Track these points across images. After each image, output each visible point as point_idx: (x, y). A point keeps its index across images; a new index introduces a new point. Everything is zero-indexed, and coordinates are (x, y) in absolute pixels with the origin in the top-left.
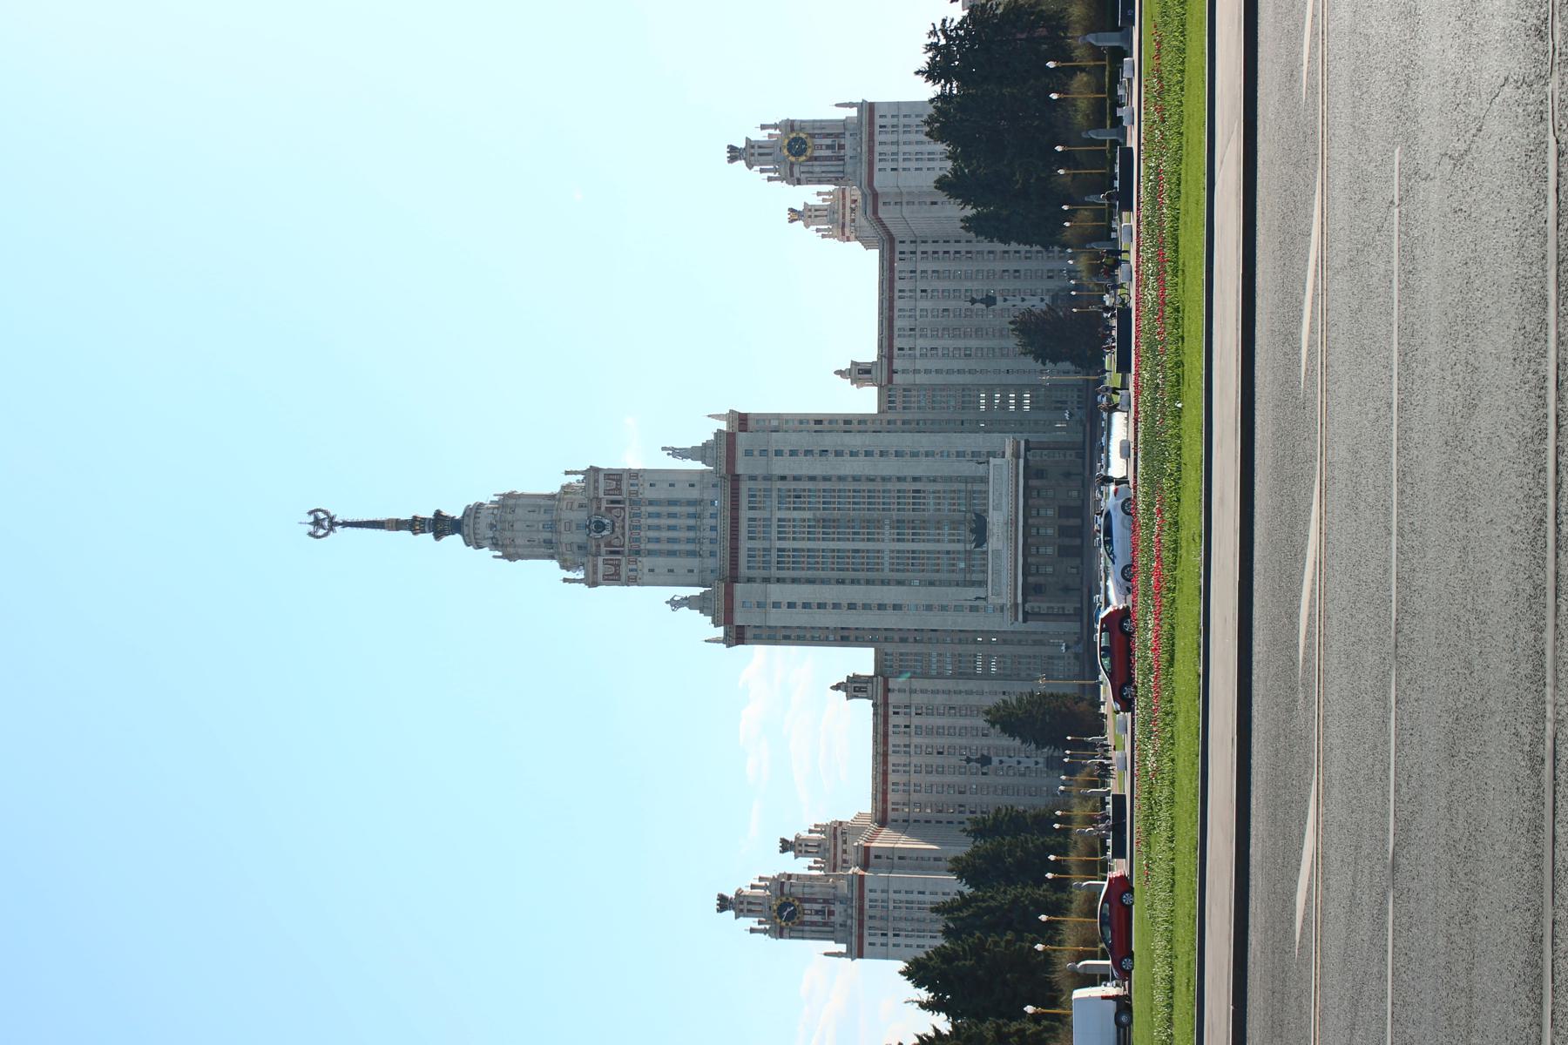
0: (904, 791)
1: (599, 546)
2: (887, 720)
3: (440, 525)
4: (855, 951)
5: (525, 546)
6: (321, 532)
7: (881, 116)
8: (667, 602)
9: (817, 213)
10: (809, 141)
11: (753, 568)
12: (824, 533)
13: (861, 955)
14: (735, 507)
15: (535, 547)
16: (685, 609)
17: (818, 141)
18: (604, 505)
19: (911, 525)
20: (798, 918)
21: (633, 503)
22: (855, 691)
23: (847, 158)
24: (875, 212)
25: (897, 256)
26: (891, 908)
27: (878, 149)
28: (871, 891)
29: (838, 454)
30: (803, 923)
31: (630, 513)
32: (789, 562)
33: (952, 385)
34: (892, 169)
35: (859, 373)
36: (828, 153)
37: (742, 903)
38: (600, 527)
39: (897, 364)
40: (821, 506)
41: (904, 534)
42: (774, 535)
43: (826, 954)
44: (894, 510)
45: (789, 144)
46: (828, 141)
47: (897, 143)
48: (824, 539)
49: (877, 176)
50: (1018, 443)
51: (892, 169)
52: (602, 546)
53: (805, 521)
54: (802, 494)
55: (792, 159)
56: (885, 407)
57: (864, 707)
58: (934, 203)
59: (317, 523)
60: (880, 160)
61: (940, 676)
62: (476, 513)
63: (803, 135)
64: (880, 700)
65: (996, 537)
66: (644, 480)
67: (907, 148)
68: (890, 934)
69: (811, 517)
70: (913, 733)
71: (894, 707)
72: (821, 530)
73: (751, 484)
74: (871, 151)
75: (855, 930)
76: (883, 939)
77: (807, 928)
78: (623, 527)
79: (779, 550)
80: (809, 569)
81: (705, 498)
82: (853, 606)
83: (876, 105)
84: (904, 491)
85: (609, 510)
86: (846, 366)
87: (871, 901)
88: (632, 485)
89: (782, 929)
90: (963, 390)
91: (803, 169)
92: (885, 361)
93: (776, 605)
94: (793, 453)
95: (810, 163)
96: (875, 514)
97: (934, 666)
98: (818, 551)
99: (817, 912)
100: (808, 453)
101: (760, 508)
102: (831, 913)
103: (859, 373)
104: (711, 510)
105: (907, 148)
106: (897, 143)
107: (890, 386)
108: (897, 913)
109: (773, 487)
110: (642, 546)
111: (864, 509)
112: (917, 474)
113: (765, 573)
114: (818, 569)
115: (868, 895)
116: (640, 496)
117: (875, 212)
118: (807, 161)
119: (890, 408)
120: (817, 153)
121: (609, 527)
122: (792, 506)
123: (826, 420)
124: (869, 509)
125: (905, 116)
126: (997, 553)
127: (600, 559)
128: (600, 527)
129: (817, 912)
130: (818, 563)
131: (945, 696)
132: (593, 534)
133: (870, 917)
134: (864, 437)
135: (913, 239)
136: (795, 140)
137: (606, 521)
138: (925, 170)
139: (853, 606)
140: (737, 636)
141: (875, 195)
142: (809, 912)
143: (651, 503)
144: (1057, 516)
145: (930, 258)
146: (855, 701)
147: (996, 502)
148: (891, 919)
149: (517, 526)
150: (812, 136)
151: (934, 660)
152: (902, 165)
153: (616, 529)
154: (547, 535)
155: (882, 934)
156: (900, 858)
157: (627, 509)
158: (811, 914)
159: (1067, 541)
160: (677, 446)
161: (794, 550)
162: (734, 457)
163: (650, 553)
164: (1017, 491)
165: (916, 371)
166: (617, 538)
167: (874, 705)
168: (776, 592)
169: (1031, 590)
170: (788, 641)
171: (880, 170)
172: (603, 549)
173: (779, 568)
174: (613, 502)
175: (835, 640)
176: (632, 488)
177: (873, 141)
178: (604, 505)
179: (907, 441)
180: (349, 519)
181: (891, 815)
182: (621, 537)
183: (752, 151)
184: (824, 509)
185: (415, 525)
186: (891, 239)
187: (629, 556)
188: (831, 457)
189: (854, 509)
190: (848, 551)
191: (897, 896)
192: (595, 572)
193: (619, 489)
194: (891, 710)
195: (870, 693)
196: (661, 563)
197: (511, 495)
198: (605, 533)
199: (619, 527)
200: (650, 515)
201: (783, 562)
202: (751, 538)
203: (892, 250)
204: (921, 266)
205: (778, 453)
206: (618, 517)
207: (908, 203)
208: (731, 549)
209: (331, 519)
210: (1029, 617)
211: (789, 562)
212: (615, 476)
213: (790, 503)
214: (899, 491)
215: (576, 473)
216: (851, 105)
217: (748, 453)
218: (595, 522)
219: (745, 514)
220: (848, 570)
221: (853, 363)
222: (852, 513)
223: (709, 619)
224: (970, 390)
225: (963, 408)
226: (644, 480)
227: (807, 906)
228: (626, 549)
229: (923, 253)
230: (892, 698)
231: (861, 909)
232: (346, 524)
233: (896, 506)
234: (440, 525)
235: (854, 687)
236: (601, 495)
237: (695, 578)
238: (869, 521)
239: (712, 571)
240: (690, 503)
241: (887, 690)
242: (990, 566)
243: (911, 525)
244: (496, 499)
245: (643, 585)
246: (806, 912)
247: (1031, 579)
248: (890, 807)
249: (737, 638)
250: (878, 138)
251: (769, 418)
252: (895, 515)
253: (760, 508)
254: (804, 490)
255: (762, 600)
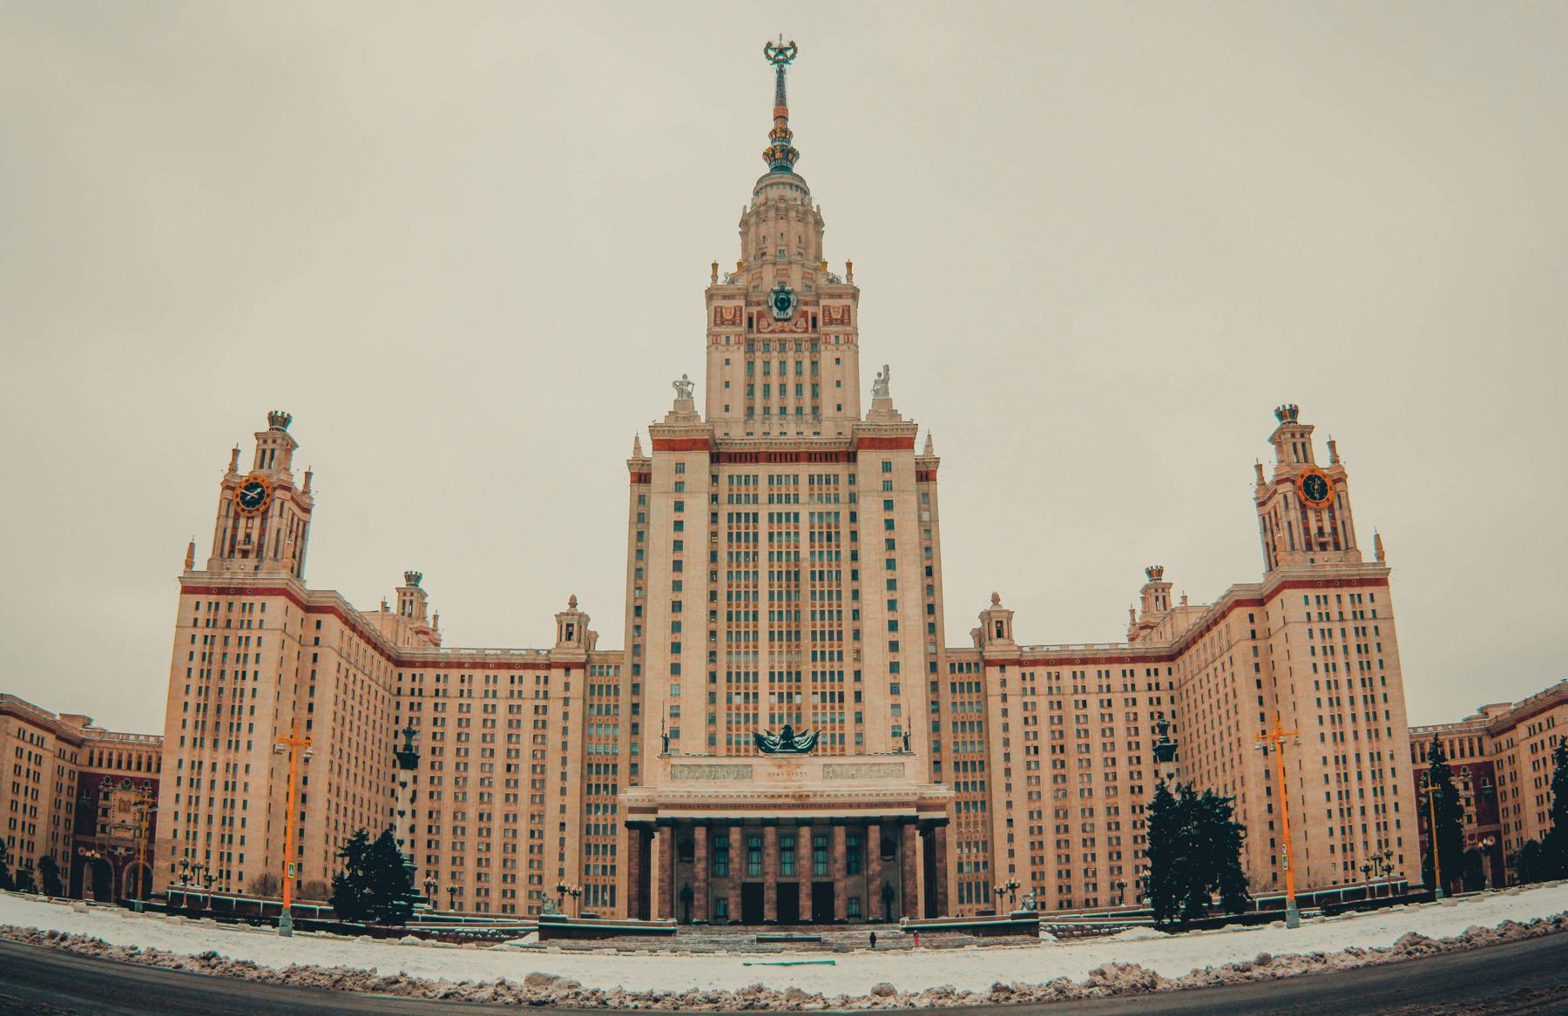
0: (437, 691)
1: (759, 304)
2: (529, 668)
3: (782, 156)
4: (189, 584)
5: (757, 234)
6: (772, 53)
7: (1372, 595)
8: (685, 377)
9: (1299, 447)
10: (1324, 504)
11: (731, 482)
12: (780, 573)
13: (186, 590)
14: (812, 457)
15: (758, 244)
16: (674, 395)
17: (1326, 516)
18: (810, 309)
19: (794, 691)
20: (243, 510)
21: (814, 344)
22: (569, 625)
23: (1310, 555)
24: (1239, 603)
25: (1152, 666)
26: (240, 633)
27: (1332, 593)
28: (263, 605)
29: (891, 585)
30: (237, 517)
31: (801, 339)
32: (739, 528)
33: (988, 748)
34: (1308, 614)
35: (996, 624)
36: (1314, 530)
37: (274, 442)
38: (783, 304)
39: (1013, 673)
40: (817, 569)
41: (781, 680)
42: (777, 508)
43: (192, 546)
44: (814, 666)
45: (1319, 478)
46: (1328, 529)
47: (1342, 619)
48: (771, 573)
49: (1298, 594)
50: (942, 807)
51: (1308, 614)
52: (759, 308)
53: (796, 547)
54: (833, 543)
55: (1300, 482)
56: (954, 659)
57: (544, 638)
58: (1259, 682)
59: (781, 51)
60: (1318, 597)
61: (586, 737)
62: (797, 187)
63: (1330, 495)
64: (555, 658)
65: (775, 770)
66: (844, 351)
67: (1337, 634)
68: (208, 632)
69: (801, 556)
70: (511, 702)
71: (546, 678)
72: (784, 569)
73: (843, 479)
74: (1328, 583)
75: (217, 582)
76: (201, 623)
77: (230, 522)
78: (782, 331)
79: (755, 515)
80: (730, 554)
81: (823, 423)
82: (676, 608)
83: (1384, 587)
84: (841, 679)
85: (805, 314)
86: (1005, 604)
87: (251, 604)
88: (837, 337)
89: (233, 489)
90: (981, 763)
91: (1290, 495)
92: (1015, 656)
93: (679, 506)
94: (890, 524)
95: (1298, 507)
96: (806, 641)
97: (602, 731)
98: (755, 566)
99: (248, 536)
100: (891, 544)
101: (812, 489)
102: (245, 554)
103: (996, 624)
104: (808, 433)
105: (1337, 634)
106: (1342, 619)
107: (981, 665)
108: (233, 641)
109: (841, 505)
110: (758, 354)
111: (814, 626)
112: (866, 697)
113: (723, 497)
114: (730, 566)
115: (257, 600)
116: (823, 347)
117: (1239, 603)
118: (1300, 502)
119: (952, 665)
120: (1311, 515)
121: (782, 317)
122: (817, 530)
123: (933, 581)
124: (814, 633)
125: (1376, 628)
126: (745, 773)
127: (742, 303)
128: (783, 304)
129: (248, 536)
130: (738, 566)
131: (560, 745)
132: (773, 297)
133: (230, 604)
134: (917, 618)
135: (1175, 686)
136: (1323, 485)
137: (790, 311)
138: (1313, 660)
139: (676, 608)
140: (641, 477)
141: (1260, 602)
142: (250, 525)
143: (814, 364)
144: (816, 880)
145: (1152, 709)
146: (555, 625)
147: (838, 770)
148: (227, 632)
149: (782, 224)
150: (1331, 509)
151: (610, 732)
152: (1316, 627)
153: (779, 323)
154: (771, 251)
155: (208, 620)
156: (315, 656)
157: (805, 335)
158: (247, 527)
159: (770, 895)
160: (892, 385)
161: (756, 535)
162: (880, 448)
163: (750, 365)
164: (859, 806)
165: (1004, 697)
166: (769, 325)
167: (549, 651)
168: (697, 509)
169: (681, 831)
170: (635, 538)
171: (1306, 597)
172: (754, 310)
173: (730, 515)
174: (814, 319)
175: (636, 599)
176: (833, 337)
177: (1341, 586)
178: (810, 309)
179: (914, 679)
180: (788, 78)
181: (407, 673)
182: (769, 329)
183: (1298, 436)
184: (813, 573)
185: (781, 133)
186: (1172, 657)
187: (747, 340)
188: (887, 575)
189: (813, 613)
190: (755, 606)
191: (253, 642)
192: (725, 297)
193: (831, 322)
194: (542, 673)
195: (565, 644)
196: (738, 372)
197: (819, 223)
198: (775, 311)
199: (782, 326)
200: (799, 363)
201: (739, 520)
202: (771, 478)
203: (1159, 659)
204: (1142, 698)
205: (889, 505)
206: (795, 325)
207: (1255, 648)
208: (757, 454)
209: (786, 61)
210: (636, 833)
211: (739, 528)
212: (846, 318)
213: (821, 527)
214: (840, 673)
215: (849, 275)
216: (1380, 555)
217: (887, 467)
218: (789, 299)
219: (804, 470)
220: (729, 605)
221: (1010, 614)
222: (809, 609)
223: (661, 420)
224: (982, 769)
225: (957, 764)
226: (844, 351)
227: (257, 522)
228: (755, 335)
229: (1159, 700)
230: (557, 675)
231: (240, 591)
232: (781, 74)
233: (819, 669)
234: (782, 156)
235: (572, 626)
236: (823, 302)
237: (717, 412)
238: (798, 633)
239: (726, 434)
240: (815, 410)
241: (568, 668)
242: (726, 761)
243: (794, 691)
244: (814, 205)
245: (709, 354)
246: (250, 521)
247: (700, 834)
248: (417, 671)
249: (640, 475)
250: (1346, 593)
251: (932, 508)
252: (807, 668)
253: (812, 489)
254: (838, 546)
255: (686, 488)
